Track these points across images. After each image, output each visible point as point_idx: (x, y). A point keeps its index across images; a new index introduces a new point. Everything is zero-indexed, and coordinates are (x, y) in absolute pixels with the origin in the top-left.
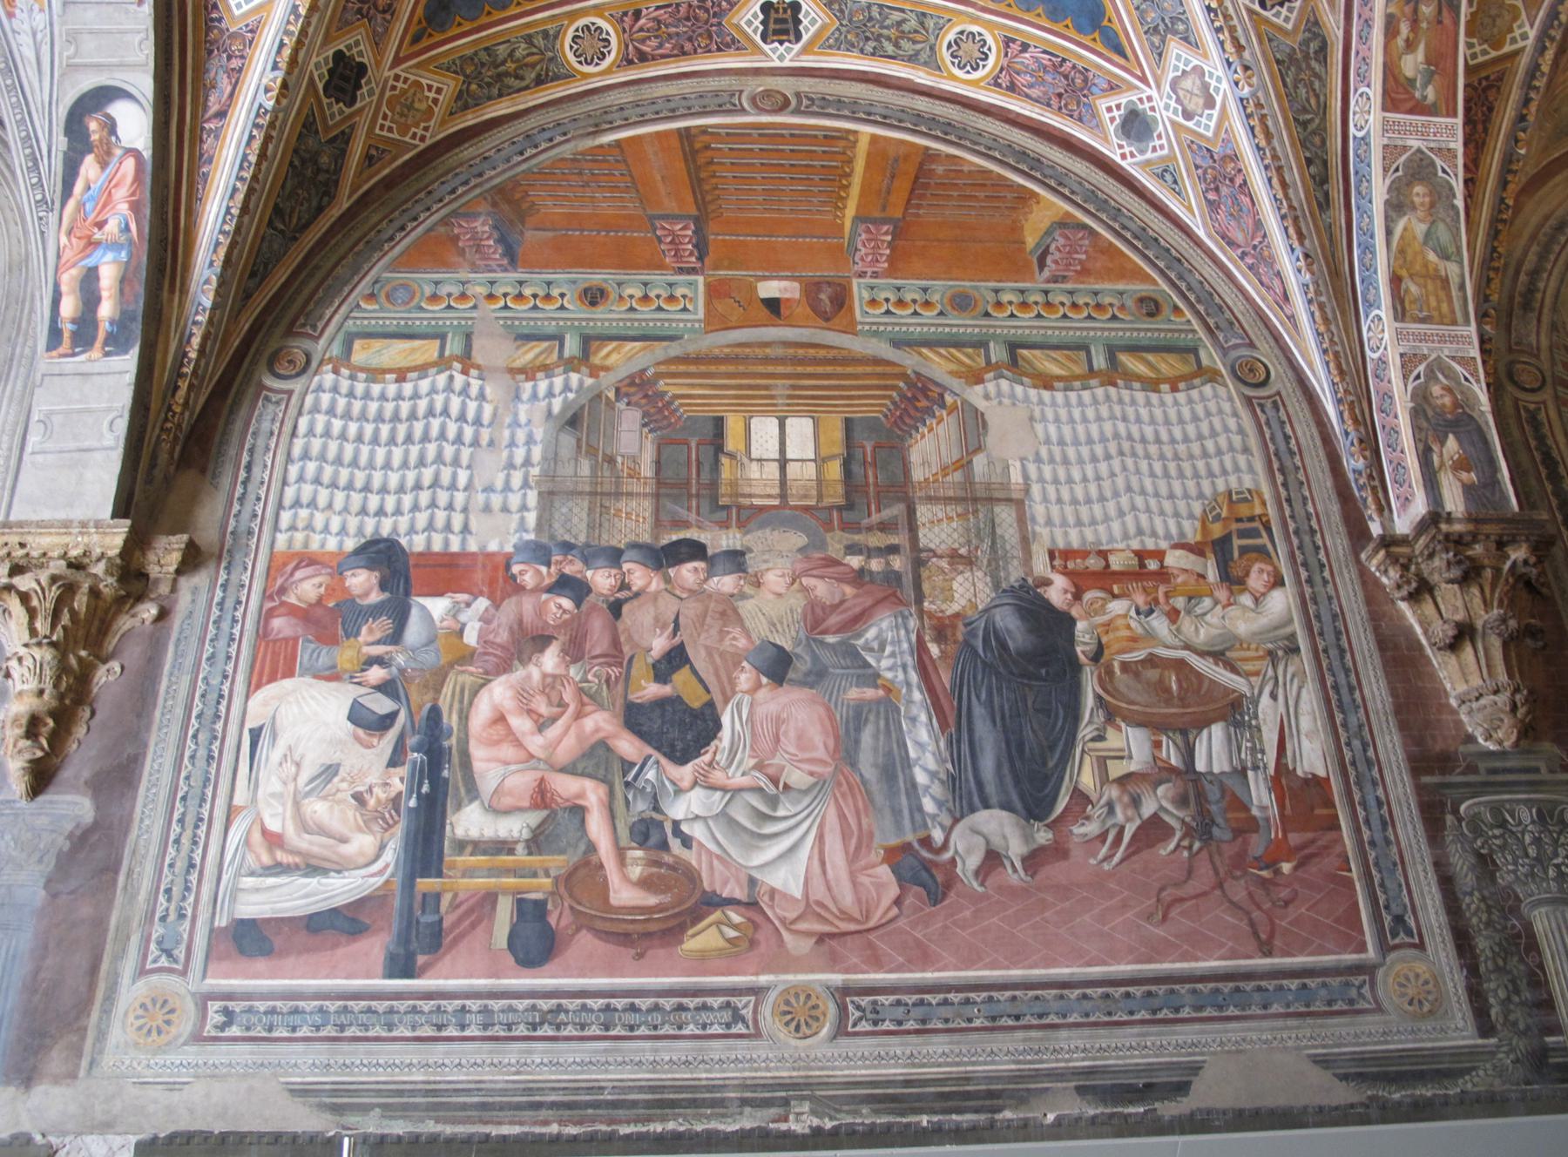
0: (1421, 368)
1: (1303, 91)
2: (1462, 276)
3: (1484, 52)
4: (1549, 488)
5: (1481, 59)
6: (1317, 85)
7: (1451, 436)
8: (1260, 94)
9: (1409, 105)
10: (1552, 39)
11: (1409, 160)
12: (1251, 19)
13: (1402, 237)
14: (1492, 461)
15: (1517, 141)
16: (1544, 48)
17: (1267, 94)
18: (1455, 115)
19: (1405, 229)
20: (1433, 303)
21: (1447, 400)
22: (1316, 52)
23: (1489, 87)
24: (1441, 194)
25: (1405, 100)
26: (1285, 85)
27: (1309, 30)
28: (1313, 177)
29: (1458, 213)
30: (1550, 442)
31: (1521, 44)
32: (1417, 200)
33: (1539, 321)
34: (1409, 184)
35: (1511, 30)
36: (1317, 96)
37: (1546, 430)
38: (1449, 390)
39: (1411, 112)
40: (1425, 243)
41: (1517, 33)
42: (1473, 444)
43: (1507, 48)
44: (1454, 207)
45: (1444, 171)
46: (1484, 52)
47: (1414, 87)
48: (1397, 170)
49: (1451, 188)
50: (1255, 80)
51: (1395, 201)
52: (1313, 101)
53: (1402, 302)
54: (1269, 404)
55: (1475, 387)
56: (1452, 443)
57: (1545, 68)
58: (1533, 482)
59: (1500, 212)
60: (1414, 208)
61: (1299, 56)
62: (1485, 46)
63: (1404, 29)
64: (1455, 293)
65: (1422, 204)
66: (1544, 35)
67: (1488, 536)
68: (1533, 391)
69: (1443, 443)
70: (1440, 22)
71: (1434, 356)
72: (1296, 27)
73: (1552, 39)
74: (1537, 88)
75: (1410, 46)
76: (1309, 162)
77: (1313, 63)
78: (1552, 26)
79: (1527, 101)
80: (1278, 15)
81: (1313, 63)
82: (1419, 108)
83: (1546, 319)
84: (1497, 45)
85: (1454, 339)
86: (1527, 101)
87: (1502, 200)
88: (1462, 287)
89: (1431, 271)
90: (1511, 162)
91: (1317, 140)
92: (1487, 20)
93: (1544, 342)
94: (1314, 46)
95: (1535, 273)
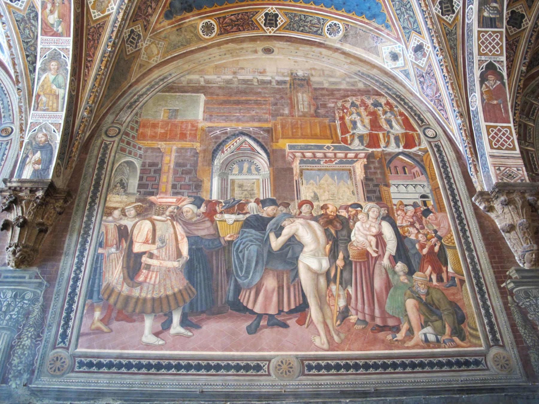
0: (37, 127)
1: (27, 31)
2: (65, 94)
3: (99, 15)
4: (96, 171)
5: (97, 17)
6: (33, 29)
7: (39, 152)
8: (8, 32)
9: (51, 33)
10: (122, 9)
11: (51, 53)
12: (6, 6)
13: (44, 81)
14: (50, 162)
15: (108, 46)
16: (119, 12)
17: (11, 33)
18: (70, 36)
19: (45, 78)
20: (50, 104)
21: (43, 139)
22: (33, 17)
23: (100, 27)
24: (61, 65)
25: (50, 32)
26: (19, 29)
27: (30, 9)
28: (29, 62)
29: (67, 72)
30: (107, 156)
31: (111, 11)
32: (52, 67)
33: (132, 112)
34: (50, 62)
35: (108, 7)
36: (34, 33)
37: (108, 152)
38: (46, 135)
39: (52, 36)
40: (53, 82)
41: (110, 7)
42: (46, 154)
43: (107, 13)
44: (67, 70)
45: (64, 56)
46: (99, 15)
47: (54, 27)
48: (45, 57)
49: (66, 63)
50: (6, 28)
51: (43, 68)
52: (31, 34)
53: (38, 104)
54: (5, 143)
55: (57, 134)
56: (38, 155)
57: (120, 20)
58: (91, 170)
59: (99, 71)
60: (50, 70)
61: (26, 18)
62: (99, 13)
63: (49, 6)
64: (60, 100)
65: (54, 69)
66: (119, 7)
67: (26, 188)
68: (112, 137)
69: (34, 154)
70: (63, 3)
71: (44, 123)
72: (25, 9)
73: (122, 9)
74: (116, 27)
75: (52, 12)
76: (27, 56)
77: (32, 21)
78: (122, 5)
79: (113, 31)
80: (17, 4)
81: (32, 21)
82: (56, 34)
83: (135, 111)
84: (103, 12)
85: (55, 117)
86: (113, 31)
87: (100, 67)
88: (64, 98)
89: (53, 93)
90: (105, 53)
91: (33, 48)
92: (99, 4)
93: (129, 119)
94: (32, 15)
95: (142, 95)
